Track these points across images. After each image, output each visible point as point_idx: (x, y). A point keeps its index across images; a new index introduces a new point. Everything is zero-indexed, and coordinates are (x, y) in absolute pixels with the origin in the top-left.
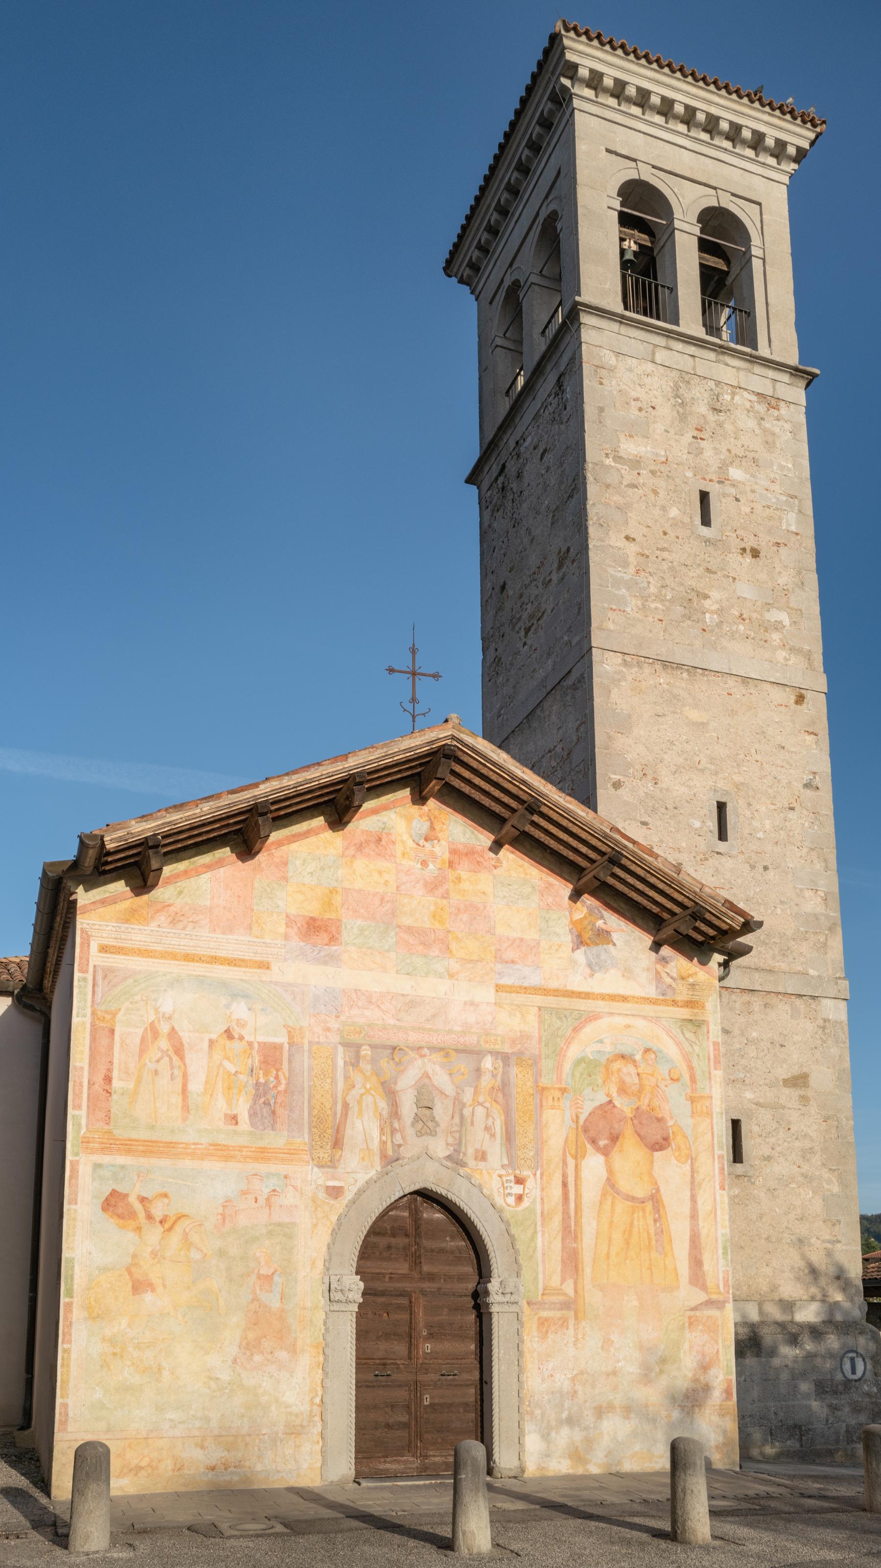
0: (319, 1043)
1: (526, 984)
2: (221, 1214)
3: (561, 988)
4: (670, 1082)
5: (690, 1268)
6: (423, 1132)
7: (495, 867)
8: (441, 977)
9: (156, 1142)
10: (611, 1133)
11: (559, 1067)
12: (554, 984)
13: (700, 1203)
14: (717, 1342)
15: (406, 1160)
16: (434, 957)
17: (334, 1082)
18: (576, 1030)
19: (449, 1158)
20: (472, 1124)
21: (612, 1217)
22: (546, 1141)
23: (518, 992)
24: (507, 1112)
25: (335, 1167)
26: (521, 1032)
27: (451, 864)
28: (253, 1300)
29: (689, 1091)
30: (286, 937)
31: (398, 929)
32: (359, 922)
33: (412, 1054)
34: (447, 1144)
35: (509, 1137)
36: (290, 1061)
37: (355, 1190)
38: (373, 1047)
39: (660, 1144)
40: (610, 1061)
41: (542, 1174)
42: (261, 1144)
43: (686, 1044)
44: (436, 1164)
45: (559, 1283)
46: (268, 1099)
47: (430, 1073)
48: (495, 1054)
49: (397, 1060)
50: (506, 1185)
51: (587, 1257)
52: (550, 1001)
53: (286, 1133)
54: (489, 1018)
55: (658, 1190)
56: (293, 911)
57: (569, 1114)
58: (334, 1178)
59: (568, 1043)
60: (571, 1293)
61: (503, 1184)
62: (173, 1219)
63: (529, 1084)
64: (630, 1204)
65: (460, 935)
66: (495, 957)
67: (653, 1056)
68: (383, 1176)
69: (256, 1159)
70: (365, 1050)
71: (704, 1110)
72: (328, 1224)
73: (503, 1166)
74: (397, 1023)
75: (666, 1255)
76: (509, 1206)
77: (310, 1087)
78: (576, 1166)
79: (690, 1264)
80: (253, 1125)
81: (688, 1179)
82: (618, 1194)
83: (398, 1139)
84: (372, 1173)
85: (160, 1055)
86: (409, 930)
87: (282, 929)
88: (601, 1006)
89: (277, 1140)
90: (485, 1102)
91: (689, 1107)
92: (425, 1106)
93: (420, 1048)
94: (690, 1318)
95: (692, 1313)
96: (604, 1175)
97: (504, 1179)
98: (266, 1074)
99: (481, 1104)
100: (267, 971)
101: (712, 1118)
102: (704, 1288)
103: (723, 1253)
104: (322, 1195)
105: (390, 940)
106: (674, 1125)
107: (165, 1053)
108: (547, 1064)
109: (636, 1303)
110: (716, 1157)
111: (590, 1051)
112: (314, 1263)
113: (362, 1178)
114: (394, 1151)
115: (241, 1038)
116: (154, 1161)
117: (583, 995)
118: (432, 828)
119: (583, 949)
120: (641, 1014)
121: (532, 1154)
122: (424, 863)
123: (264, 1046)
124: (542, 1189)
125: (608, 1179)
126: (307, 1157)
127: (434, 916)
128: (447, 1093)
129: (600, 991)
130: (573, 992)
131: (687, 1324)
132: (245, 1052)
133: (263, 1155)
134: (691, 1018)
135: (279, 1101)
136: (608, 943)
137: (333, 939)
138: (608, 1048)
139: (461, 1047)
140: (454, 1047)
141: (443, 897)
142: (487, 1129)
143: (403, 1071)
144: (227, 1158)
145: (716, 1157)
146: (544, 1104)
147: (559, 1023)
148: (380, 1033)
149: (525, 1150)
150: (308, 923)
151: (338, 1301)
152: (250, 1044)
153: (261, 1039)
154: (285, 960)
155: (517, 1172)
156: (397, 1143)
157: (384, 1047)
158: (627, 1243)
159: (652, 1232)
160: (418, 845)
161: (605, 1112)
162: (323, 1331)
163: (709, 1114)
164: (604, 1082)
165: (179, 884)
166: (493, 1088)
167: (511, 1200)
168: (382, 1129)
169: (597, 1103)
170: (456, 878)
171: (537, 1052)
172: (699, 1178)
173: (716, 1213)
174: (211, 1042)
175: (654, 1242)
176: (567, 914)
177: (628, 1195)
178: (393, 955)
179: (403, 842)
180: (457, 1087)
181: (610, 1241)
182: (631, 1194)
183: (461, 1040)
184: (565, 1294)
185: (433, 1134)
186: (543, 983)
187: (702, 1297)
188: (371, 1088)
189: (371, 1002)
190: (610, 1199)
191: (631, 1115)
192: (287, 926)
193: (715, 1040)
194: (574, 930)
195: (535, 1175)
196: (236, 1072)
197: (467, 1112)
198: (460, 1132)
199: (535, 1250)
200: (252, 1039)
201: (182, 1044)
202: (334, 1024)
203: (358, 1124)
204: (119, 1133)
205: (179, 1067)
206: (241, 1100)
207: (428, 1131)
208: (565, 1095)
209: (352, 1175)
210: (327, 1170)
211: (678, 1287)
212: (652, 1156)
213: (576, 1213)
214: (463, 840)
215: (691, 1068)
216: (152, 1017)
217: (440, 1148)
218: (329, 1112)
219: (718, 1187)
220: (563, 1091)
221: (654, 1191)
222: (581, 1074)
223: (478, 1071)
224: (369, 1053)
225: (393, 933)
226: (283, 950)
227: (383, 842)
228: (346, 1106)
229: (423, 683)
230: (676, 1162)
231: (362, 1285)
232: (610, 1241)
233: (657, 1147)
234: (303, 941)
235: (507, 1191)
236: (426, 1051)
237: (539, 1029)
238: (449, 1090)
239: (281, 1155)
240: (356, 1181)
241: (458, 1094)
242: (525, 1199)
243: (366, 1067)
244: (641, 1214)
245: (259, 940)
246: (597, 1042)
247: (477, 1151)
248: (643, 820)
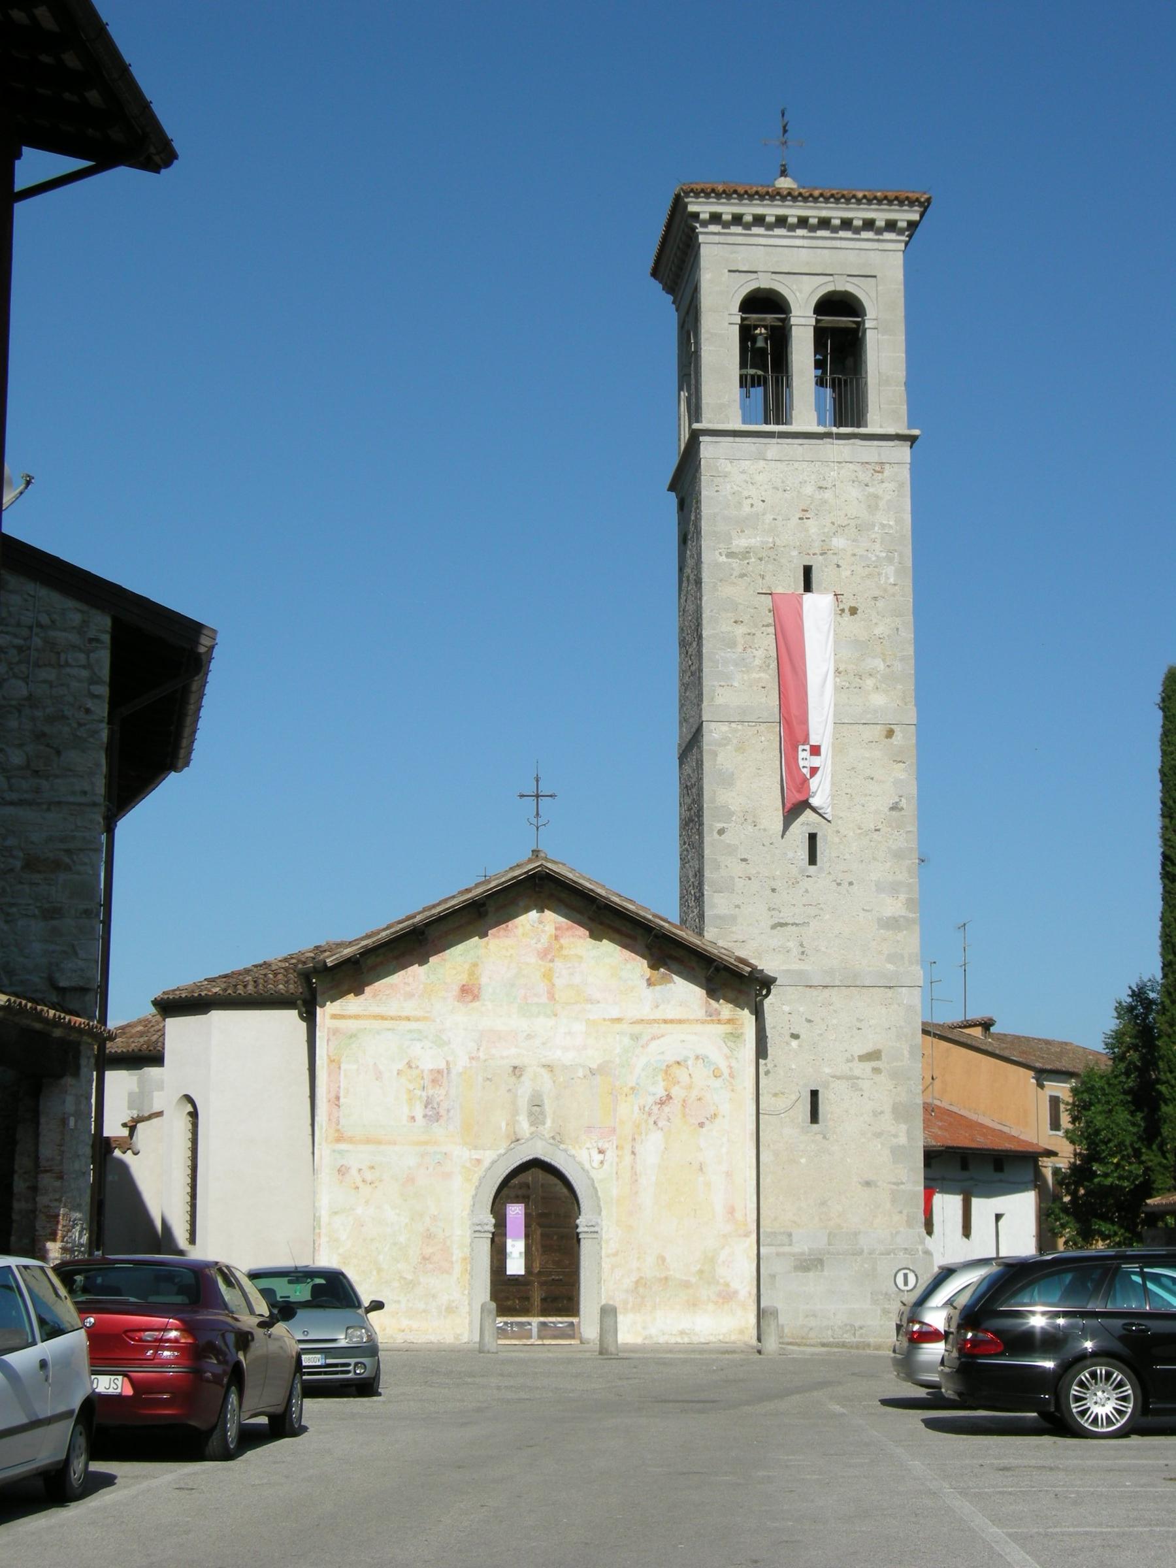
15: (523, 1141)
76: (593, 1168)
115: (417, 1067)
137: (476, 997)
160: (533, 926)
229: (543, 802)
231: (493, 1221)
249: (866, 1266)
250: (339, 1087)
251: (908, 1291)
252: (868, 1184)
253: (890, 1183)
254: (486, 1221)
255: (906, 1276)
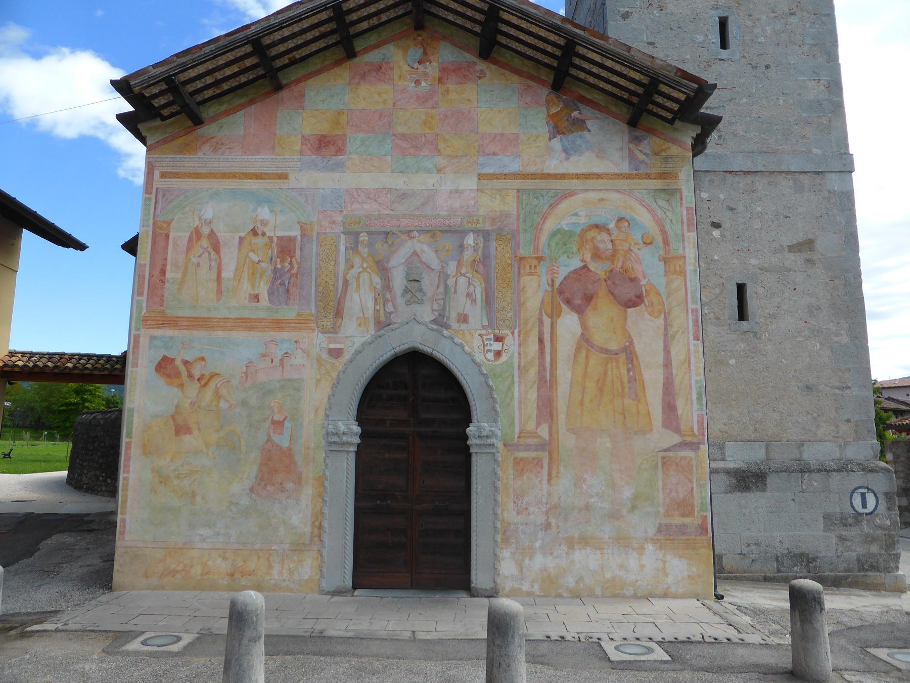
0: (325, 233)
1: (506, 172)
2: (245, 373)
3: (538, 172)
4: (643, 245)
5: (664, 412)
6: (411, 301)
7: (480, 78)
8: (429, 171)
9: (196, 318)
10: (585, 294)
11: (536, 238)
12: (532, 169)
13: (673, 352)
14: (691, 481)
15: (396, 325)
16: (424, 157)
17: (336, 262)
18: (552, 206)
19: (434, 321)
20: (455, 292)
21: (586, 367)
22: (524, 304)
23: (498, 179)
24: (487, 280)
25: (336, 333)
26: (500, 211)
27: (440, 81)
28: (268, 441)
29: (662, 253)
30: (301, 153)
31: (394, 137)
32: (361, 135)
33: (404, 237)
34: (433, 310)
35: (489, 302)
36: (301, 250)
37: (353, 351)
38: (369, 233)
39: (635, 301)
40: (584, 231)
41: (519, 332)
42: (277, 316)
43: (660, 213)
44: (424, 327)
45: (534, 427)
46: (283, 281)
47: (418, 251)
48: (476, 232)
49: (390, 242)
50: (486, 343)
51: (561, 404)
52: (528, 184)
53: (297, 307)
54: (472, 202)
55: (631, 343)
56: (307, 131)
57: (544, 279)
58: (335, 342)
59: (545, 218)
60: (546, 436)
61: (483, 342)
62: (209, 377)
63: (507, 255)
64: (603, 356)
65: (447, 137)
66: (478, 152)
67: (626, 224)
68: (376, 339)
69: (273, 329)
70: (363, 236)
71: (678, 269)
72: (330, 378)
73: (483, 327)
74: (391, 212)
75: (639, 401)
76: (488, 360)
77: (317, 269)
78: (552, 324)
79: (663, 408)
80: (271, 301)
81: (661, 331)
82: (592, 348)
83: (390, 307)
84: (367, 337)
85: (202, 251)
86: (404, 136)
87: (298, 147)
88: (575, 184)
89: (289, 313)
90: (467, 272)
91: (662, 267)
92: (414, 281)
93: (409, 232)
94: (663, 458)
95: (664, 454)
96: (578, 330)
97: (485, 337)
98: (283, 261)
99: (464, 275)
100: (285, 181)
101: (685, 276)
102: (677, 430)
103: (698, 399)
104: (325, 355)
105: (387, 146)
106: (647, 283)
107: (205, 249)
108: (524, 237)
109: (609, 445)
110: (690, 311)
111: (565, 225)
112: (317, 411)
113: (359, 341)
114: (386, 317)
115: (264, 234)
116: (196, 333)
117: (559, 177)
118: (425, 53)
119: (559, 137)
120: (615, 188)
121: (510, 315)
122: (417, 82)
123: (281, 238)
124: (520, 345)
125: (582, 334)
126: (313, 326)
127: (425, 124)
128: (433, 267)
129: (575, 172)
130: (549, 175)
131: (660, 464)
132: (266, 245)
133: (278, 324)
134: (666, 188)
135: (291, 281)
136: (583, 130)
137: (340, 151)
138: (583, 220)
139: (447, 228)
140: (440, 229)
141: (433, 107)
142: (468, 295)
143: (395, 251)
144: (251, 329)
145: (690, 311)
146: (522, 271)
147: (536, 202)
148: (376, 222)
149: (504, 312)
150: (320, 141)
151: (334, 443)
152: (271, 238)
153: (279, 234)
154: (301, 170)
155: (497, 331)
156: (389, 311)
157: (380, 233)
158: (601, 390)
159: (625, 380)
161: (580, 275)
162: (323, 467)
163: (683, 273)
164: (579, 249)
165: (220, 121)
166: (474, 261)
167: (491, 356)
168: (376, 300)
169: (572, 268)
170: (445, 91)
171: (515, 228)
172: (671, 333)
173: (689, 362)
174: (241, 239)
175: (627, 389)
176: (545, 109)
177: (602, 348)
178: (389, 158)
179: (400, 67)
180: (442, 262)
181: (584, 389)
182: (605, 347)
183: (447, 222)
184: (540, 437)
185: (421, 302)
186: (521, 169)
187: (677, 439)
188: (367, 267)
189: (369, 197)
190: (584, 353)
191: (604, 277)
192: (302, 144)
193: (688, 205)
194: (551, 122)
195: (513, 333)
196: (259, 261)
197: (451, 282)
198: (444, 299)
199: (512, 399)
200: (272, 234)
201: (218, 242)
202: (339, 218)
203: (356, 297)
204: (170, 313)
205: (216, 260)
206: (261, 284)
207: (416, 300)
208: (542, 263)
209: (351, 339)
210: (329, 335)
211: (651, 430)
212: (626, 312)
213: (551, 365)
214: (451, 59)
215: (663, 232)
216: (197, 223)
217: (426, 313)
218: (332, 288)
219: (691, 338)
220: (540, 259)
221: (627, 344)
222: (557, 244)
223: (462, 247)
224: (367, 238)
225: (389, 141)
226: (299, 163)
227: (383, 70)
228: (346, 283)
230: (649, 317)
231: (357, 429)
232: (584, 389)
233: (630, 304)
234: (315, 154)
235: (486, 348)
236: (415, 233)
237: (518, 208)
238: (435, 264)
239: (292, 325)
240: (354, 344)
241: (443, 267)
242: (504, 354)
243: (364, 250)
244: (614, 364)
245: (280, 157)
246: (572, 215)
247: (459, 314)
248: (650, 40)
249: (815, 484)
250: (166, 259)
251: (867, 514)
252: (808, 388)
253: (832, 387)
254: (342, 427)
255: (863, 495)
